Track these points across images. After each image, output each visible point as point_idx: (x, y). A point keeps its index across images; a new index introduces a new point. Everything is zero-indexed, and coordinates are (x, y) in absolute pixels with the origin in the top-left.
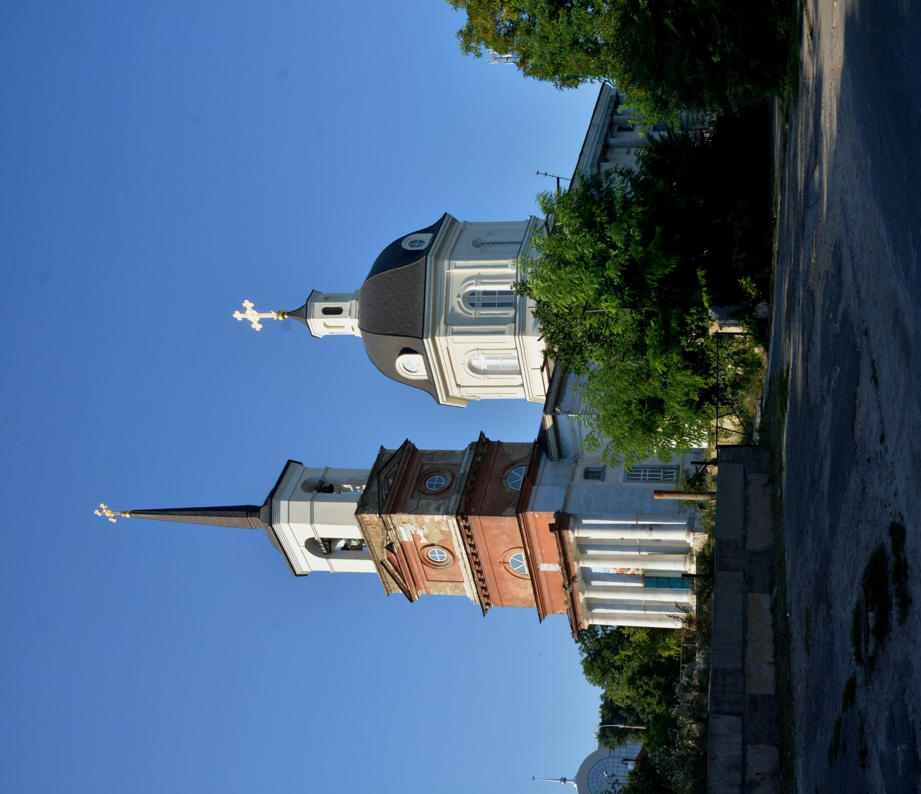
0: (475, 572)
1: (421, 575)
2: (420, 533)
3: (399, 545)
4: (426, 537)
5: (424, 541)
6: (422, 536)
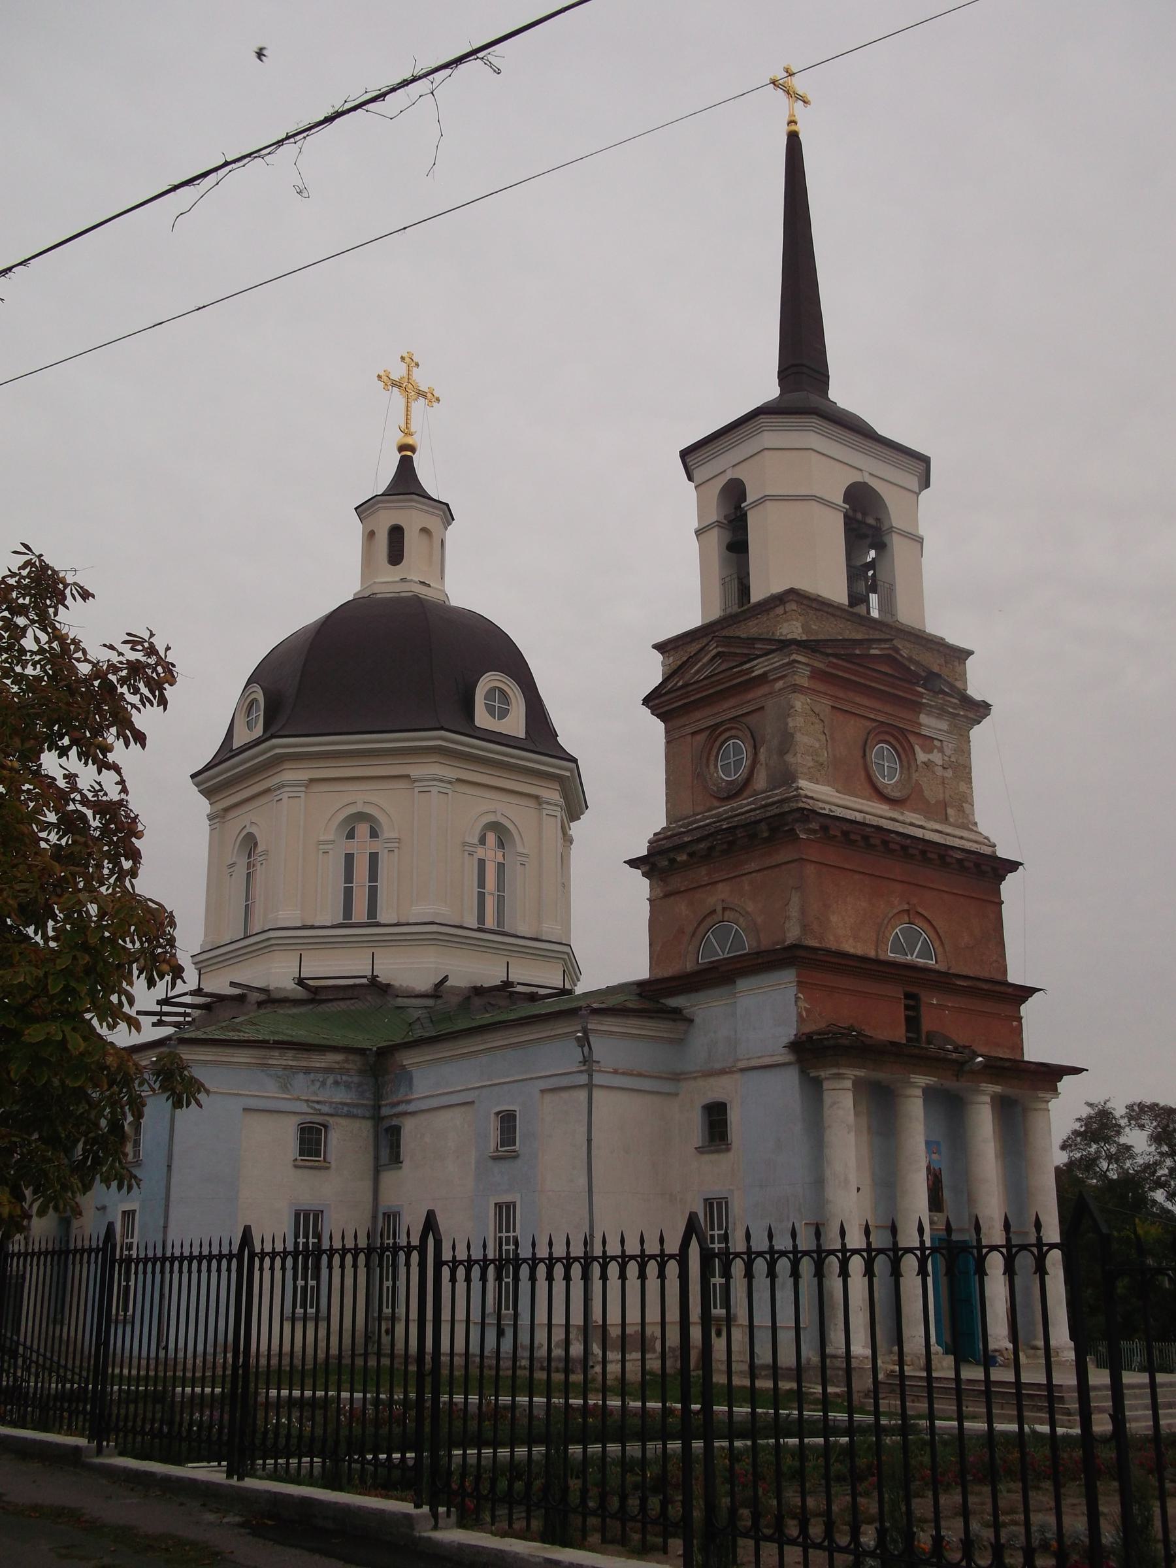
0: (909, 841)
1: (846, 701)
2: (936, 757)
3: (924, 701)
4: (928, 765)
5: (922, 756)
6: (931, 757)
